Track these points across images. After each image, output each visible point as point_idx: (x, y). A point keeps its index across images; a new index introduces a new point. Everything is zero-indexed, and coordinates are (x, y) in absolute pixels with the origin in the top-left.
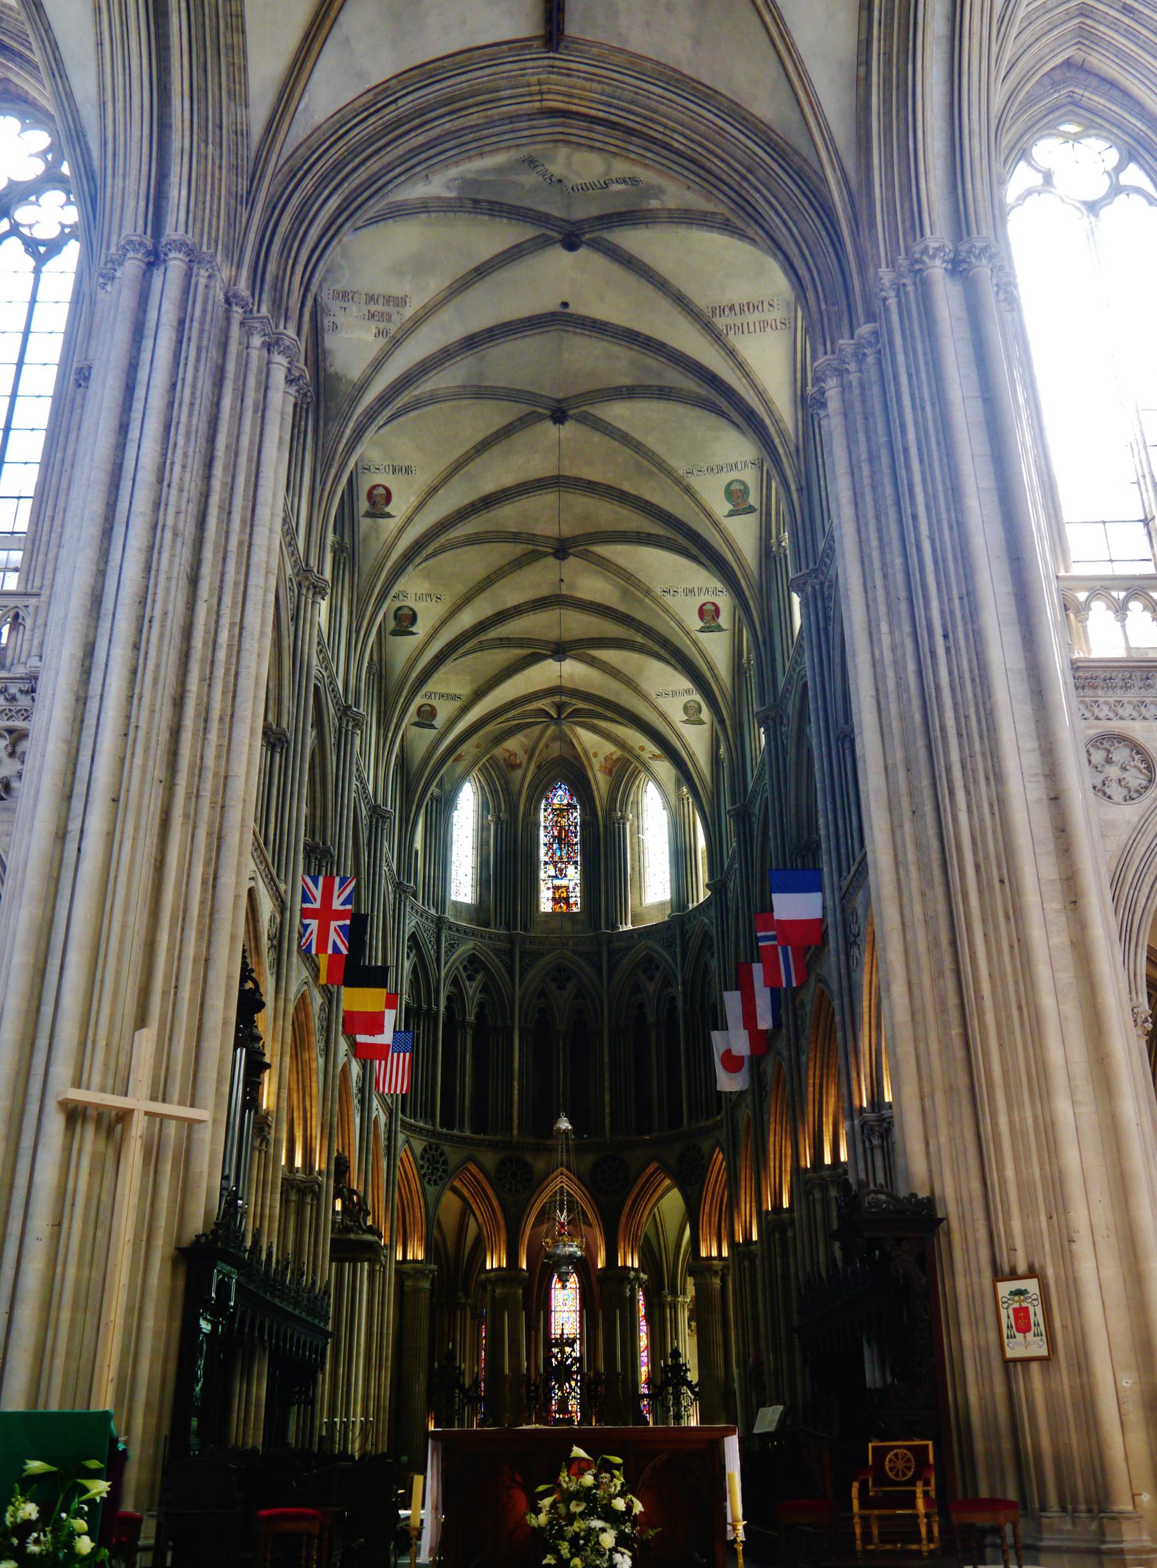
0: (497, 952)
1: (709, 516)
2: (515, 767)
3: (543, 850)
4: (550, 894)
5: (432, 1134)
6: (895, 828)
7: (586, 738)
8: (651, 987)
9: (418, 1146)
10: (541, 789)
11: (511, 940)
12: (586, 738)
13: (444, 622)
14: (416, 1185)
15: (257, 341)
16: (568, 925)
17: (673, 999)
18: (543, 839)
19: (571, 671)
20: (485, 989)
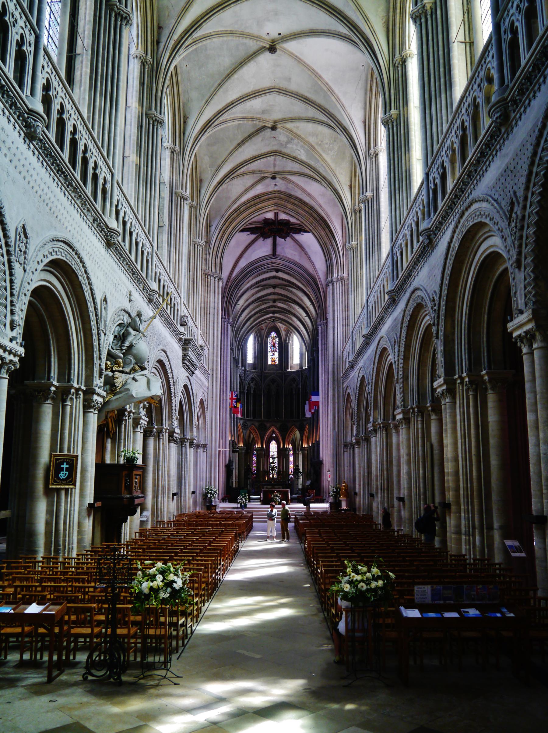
0: (258, 376)
1: (306, 305)
2: (262, 329)
3: (269, 348)
4: (271, 360)
5: (245, 419)
6: (322, 407)
7: (280, 324)
8: (294, 385)
9: (241, 422)
10: (268, 334)
11: (261, 373)
12: (280, 325)
13: (248, 314)
14: (241, 431)
15: (226, 323)
16: (275, 368)
17: (299, 388)
18: (269, 345)
19: (276, 315)
20: (255, 384)
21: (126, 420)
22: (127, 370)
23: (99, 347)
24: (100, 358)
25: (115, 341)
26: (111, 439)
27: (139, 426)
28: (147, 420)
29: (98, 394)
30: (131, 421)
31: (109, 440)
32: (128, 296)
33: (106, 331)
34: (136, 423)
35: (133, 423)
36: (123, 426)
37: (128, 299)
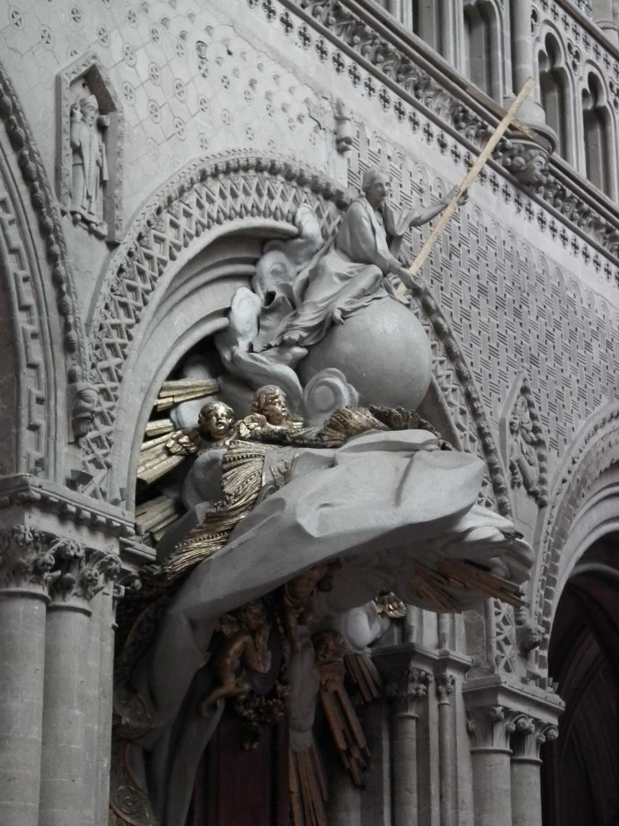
21: (423, 700)
22: (313, 431)
23: (60, 294)
24: (69, 347)
25: (270, 321)
26: (361, 788)
27: (499, 731)
28: (557, 701)
29: (62, 512)
30: (457, 705)
31: (351, 799)
32: (330, 123)
33: (113, 226)
34: (482, 712)
35: (468, 714)
36: (411, 726)
37: (331, 138)
